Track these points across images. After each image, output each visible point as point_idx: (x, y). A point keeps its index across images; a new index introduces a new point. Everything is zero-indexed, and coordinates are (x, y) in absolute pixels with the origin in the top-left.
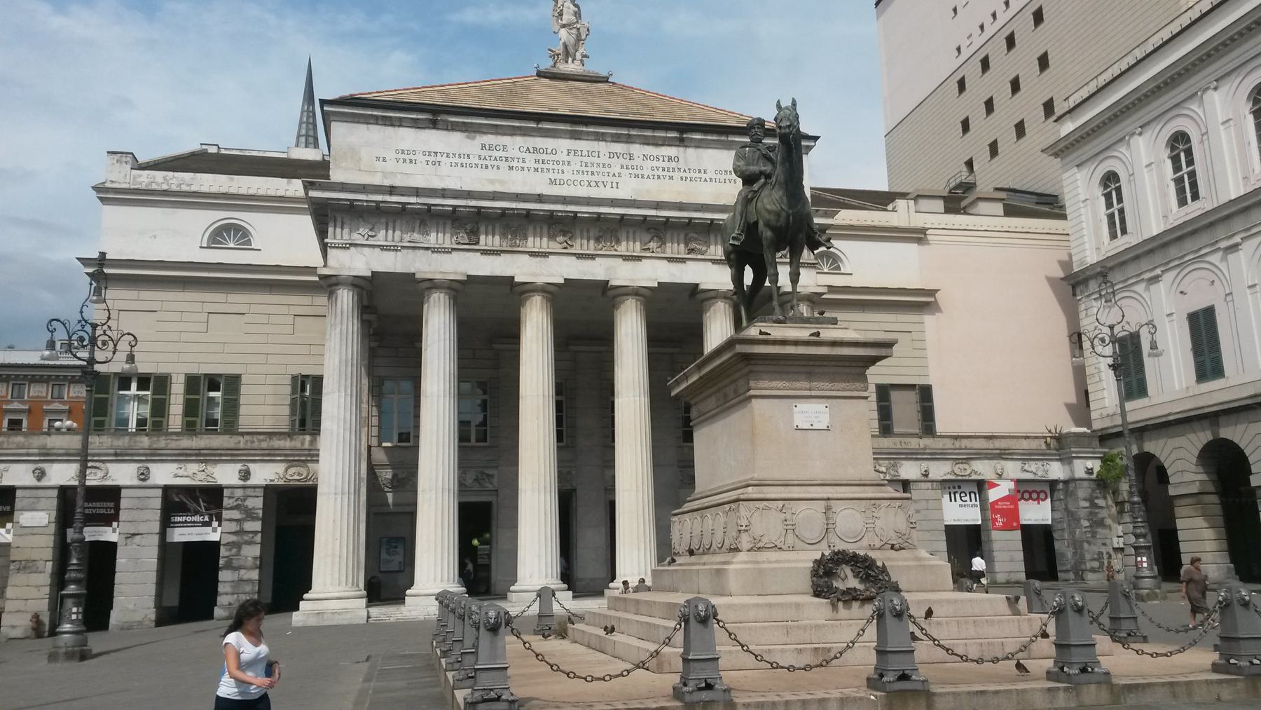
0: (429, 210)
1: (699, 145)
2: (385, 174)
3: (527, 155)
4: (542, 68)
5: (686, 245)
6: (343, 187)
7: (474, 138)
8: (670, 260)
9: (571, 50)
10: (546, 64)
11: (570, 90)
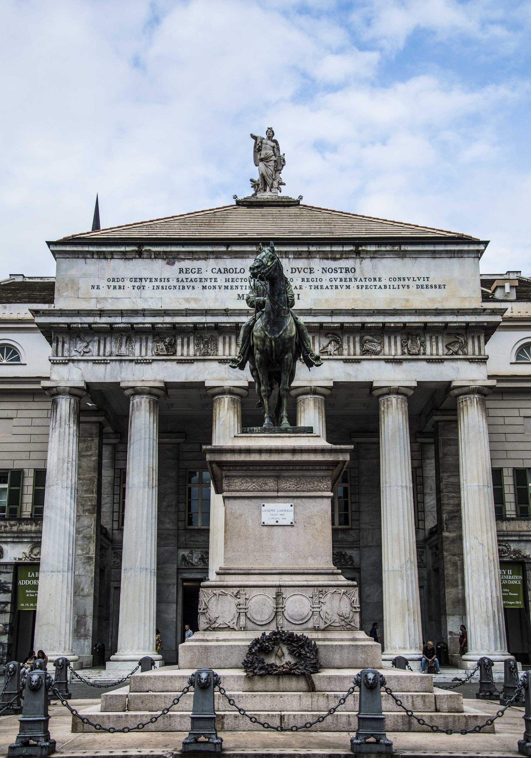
0: (132, 328)
1: (374, 255)
2: (98, 300)
3: (219, 276)
4: (240, 198)
5: (362, 346)
6: (62, 313)
7: (173, 264)
8: (346, 361)
9: (269, 181)
10: (247, 192)
11: (263, 215)
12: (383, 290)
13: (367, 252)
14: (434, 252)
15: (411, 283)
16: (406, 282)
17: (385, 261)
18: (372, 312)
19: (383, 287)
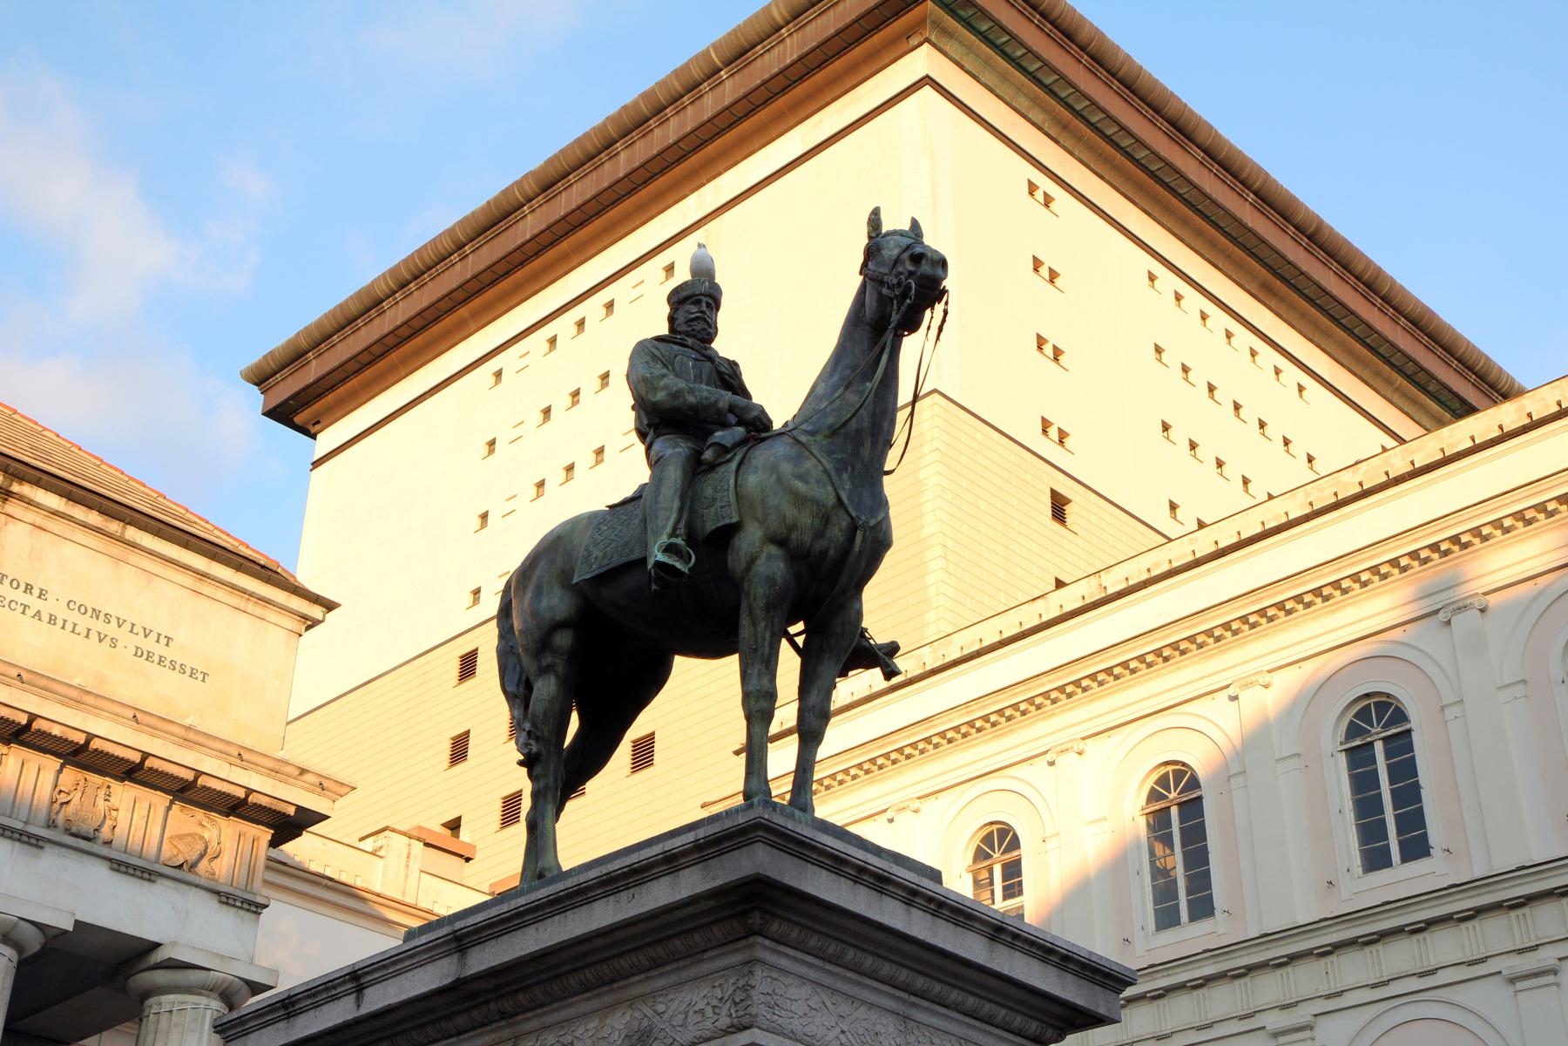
12: (44, 624)
13: (30, 502)
14: (204, 575)
15: (123, 635)
16: (111, 630)
17: (69, 550)
18: (14, 673)
19: (45, 618)
